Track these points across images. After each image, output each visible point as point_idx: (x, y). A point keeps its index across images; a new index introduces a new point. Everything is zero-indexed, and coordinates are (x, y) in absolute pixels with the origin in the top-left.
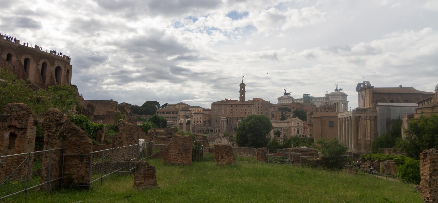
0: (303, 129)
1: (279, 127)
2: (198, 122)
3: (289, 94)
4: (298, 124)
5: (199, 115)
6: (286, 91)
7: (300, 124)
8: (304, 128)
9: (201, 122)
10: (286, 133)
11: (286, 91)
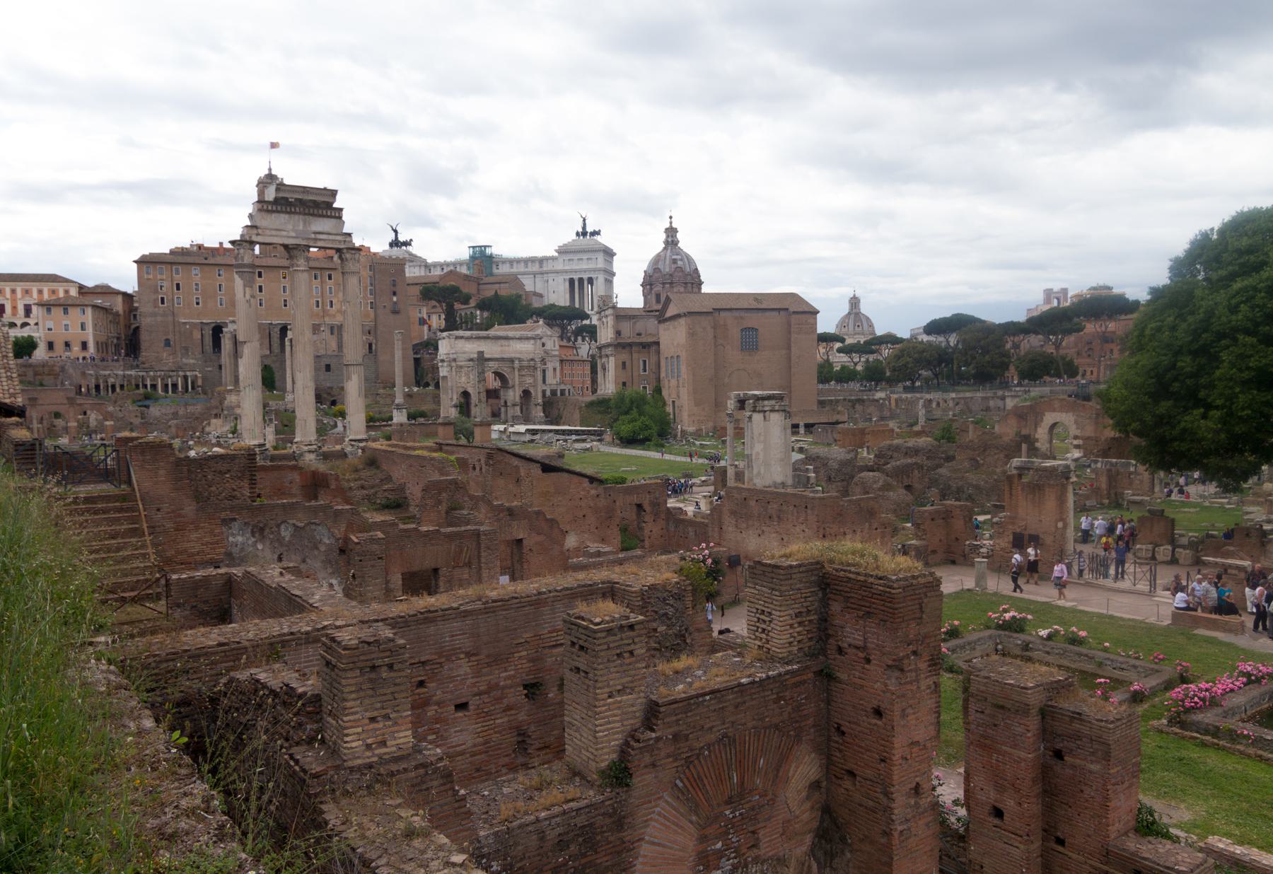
0: (558, 365)
1: (502, 359)
2: (67, 344)
3: (407, 244)
4: (543, 345)
5: (75, 313)
6: (396, 231)
7: (549, 345)
8: (562, 361)
9: (84, 346)
10: (529, 380)
11: (396, 231)
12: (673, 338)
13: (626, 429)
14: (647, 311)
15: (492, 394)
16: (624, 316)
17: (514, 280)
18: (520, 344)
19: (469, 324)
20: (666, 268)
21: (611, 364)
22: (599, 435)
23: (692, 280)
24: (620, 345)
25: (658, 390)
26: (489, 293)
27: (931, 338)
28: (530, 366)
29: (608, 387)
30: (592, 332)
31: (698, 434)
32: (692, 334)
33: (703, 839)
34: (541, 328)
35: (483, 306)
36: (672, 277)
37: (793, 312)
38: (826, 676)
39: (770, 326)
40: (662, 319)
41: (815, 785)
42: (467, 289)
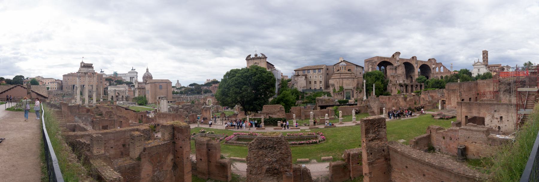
12: (148, 87)
13: (140, 103)
14: (143, 82)
15: (117, 96)
16: (139, 83)
17: (121, 77)
18: (122, 88)
19: (113, 85)
20: (147, 75)
21: (137, 91)
22: (135, 104)
23: (151, 77)
24: (139, 88)
25: (145, 96)
26: (116, 79)
27: (191, 87)
28: (123, 92)
29: (137, 95)
30: (134, 86)
31: (152, 103)
32: (151, 86)
33: (153, 168)
34: (125, 85)
35: (115, 82)
36: (148, 77)
37: (168, 83)
38: (174, 143)
39: (164, 85)
40: (146, 84)
41: (172, 159)
42: (113, 79)
